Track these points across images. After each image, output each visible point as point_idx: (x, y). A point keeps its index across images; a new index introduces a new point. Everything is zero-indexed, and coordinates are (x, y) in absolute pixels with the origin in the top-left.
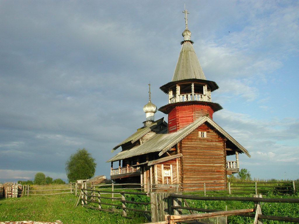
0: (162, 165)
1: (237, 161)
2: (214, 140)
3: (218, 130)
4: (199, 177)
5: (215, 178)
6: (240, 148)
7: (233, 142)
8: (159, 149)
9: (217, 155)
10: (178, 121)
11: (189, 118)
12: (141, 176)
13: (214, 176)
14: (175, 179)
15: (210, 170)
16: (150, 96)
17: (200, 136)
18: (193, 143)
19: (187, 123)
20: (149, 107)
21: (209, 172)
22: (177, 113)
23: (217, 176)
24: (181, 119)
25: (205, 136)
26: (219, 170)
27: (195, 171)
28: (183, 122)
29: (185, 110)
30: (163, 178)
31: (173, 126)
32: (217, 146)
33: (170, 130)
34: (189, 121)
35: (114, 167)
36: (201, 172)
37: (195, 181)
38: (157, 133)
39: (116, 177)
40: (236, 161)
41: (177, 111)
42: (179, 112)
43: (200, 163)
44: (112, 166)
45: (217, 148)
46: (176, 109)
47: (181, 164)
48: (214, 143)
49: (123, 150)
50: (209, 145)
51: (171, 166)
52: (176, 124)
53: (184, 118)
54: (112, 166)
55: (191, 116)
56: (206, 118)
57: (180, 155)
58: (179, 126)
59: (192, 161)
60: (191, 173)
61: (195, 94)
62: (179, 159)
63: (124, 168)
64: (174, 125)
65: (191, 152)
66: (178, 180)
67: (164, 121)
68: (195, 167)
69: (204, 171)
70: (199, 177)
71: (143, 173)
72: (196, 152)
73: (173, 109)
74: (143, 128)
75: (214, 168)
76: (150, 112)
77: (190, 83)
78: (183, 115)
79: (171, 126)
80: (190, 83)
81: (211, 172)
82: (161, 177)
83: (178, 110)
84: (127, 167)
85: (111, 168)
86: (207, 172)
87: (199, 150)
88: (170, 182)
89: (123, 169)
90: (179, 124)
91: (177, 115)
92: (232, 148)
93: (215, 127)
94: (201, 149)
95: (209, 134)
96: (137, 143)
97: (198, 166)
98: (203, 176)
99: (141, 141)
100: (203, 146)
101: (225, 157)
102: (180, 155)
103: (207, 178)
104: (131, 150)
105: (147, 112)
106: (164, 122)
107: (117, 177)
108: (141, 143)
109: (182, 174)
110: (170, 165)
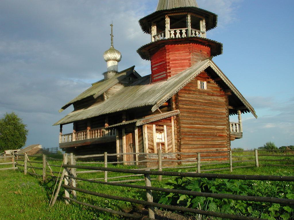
0: (154, 126)
1: (239, 122)
2: (215, 93)
3: (223, 79)
5: (218, 145)
6: (246, 106)
7: (239, 97)
8: (150, 101)
9: (219, 114)
10: (169, 66)
11: (185, 61)
12: (118, 142)
13: (216, 142)
14: (170, 147)
15: (212, 134)
16: (112, 40)
17: (199, 87)
18: (191, 96)
19: (182, 68)
20: (112, 54)
23: (219, 143)
24: (174, 62)
25: (205, 88)
26: (222, 134)
27: (194, 135)
29: (179, 51)
30: (155, 145)
31: (161, 72)
32: (218, 102)
34: (185, 66)
35: (64, 132)
36: (202, 137)
37: (194, 148)
38: (126, 85)
40: (239, 123)
42: (170, 53)
43: (200, 124)
44: (61, 130)
45: (218, 104)
46: (166, 48)
47: (177, 125)
48: (216, 98)
50: (209, 100)
51: (165, 126)
52: (166, 70)
53: (177, 62)
54: (61, 130)
55: (187, 59)
56: (209, 61)
58: (170, 72)
59: (191, 121)
60: (190, 138)
62: (175, 118)
63: (82, 133)
64: (164, 71)
66: (174, 147)
67: (135, 71)
68: (194, 129)
69: (204, 135)
70: (198, 143)
71: (121, 138)
72: (196, 109)
73: (161, 49)
74: (102, 81)
75: (216, 132)
76: (114, 60)
77: (184, 14)
78: (176, 57)
80: (184, 14)
81: (213, 137)
82: (152, 144)
83: (169, 49)
84: (88, 131)
85: (60, 133)
86: (208, 137)
87: (198, 106)
89: (80, 134)
90: (170, 69)
92: (237, 105)
93: (219, 75)
94: (201, 105)
95: (210, 85)
96: (101, 98)
97: (198, 128)
98: (204, 143)
100: (203, 101)
101: (228, 117)
102: (177, 112)
103: (208, 144)
105: (109, 60)
106: (134, 71)
108: (106, 99)
110: (163, 126)
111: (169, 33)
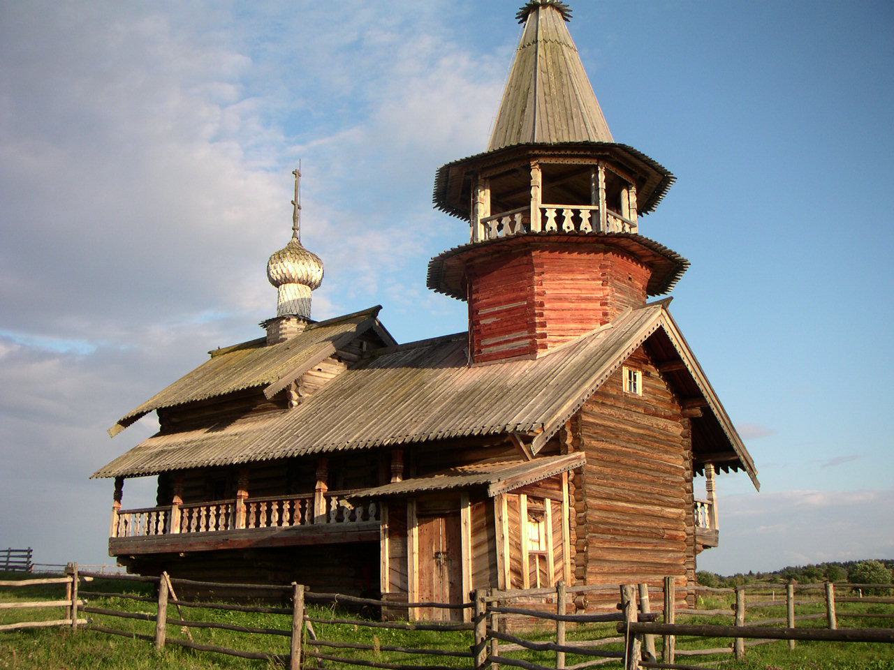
0: (524, 497)
1: (711, 500)
2: (661, 407)
3: (690, 368)
4: (624, 557)
5: (665, 564)
6: (738, 452)
7: (722, 423)
8: (518, 419)
9: (670, 473)
10: (541, 315)
11: (591, 305)
12: (385, 545)
13: (664, 555)
14: (559, 565)
15: (654, 531)
16: (295, 219)
17: (626, 387)
18: (607, 411)
19: (580, 326)
20: (301, 262)
21: (651, 540)
22: (536, 278)
23: (669, 559)
24: (557, 305)
25: (639, 391)
26: (674, 533)
27: (616, 532)
28: (562, 320)
29: (572, 272)
30: (526, 559)
31: (509, 332)
32: (667, 435)
33: (485, 351)
34: (589, 320)
35: (126, 504)
36: (631, 539)
37: (614, 574)
38: (352, 365)
39: (159, 545)
40: (710, 502)
41: (537, 270)
42: (545, 276)
43: (628, 501)
44: (118, 496)
45: (667, 443)
46: (535, 261)
47: (577, 501)
48: (662, 423)
49: (164, 431)
50: (648, 428)
51: (548, 501)
52: (532, 326)
53: (567, 305)
54: (118, 496)
55: (597, 299)
56: (659, 313)
57: (577, 458)
58: (544, 336)
59: (607, 490)
60: (605, 541)
61: (610, 211)
62: (571, 477)
63: (213, 509)
64: (522, 329)
65: (604, 451)
66: (568, 568)
67: (380, 323)
68: (614, 515)
69: (636, 534)
70: (624, 557)
71: (399, 533)
72: (619, 453)
73: (514, 262)
74: (261, 343)
75: (663, 525)
76: (301, 282)
77: (588, 162)
78: (563, 291)
79: (492, 335)
80: (588, 162)
81: (655, 541)
82: (518, 555)
83: (541, 265)
84: (241, 505)
85: (116, 504)
86: (645, 540)
87: (624, 444)
88: (544, 576)
89: (204, 513)
90: (543, 325)
91: (536, 289)
92: (714, 446)
93: (682, 355)
94: (629, 441)
95: (650, 382)
96: (282, 401)
97: (623, 512)
98: (635, 557)
99: (293, 392)
100: (635, 430)
101: (689, 481)
102: (579, 458)
103: (644, 563)
104: (232, 430)
105: (287, 280)
106: (377, 324)
107: (144, 545)
108: (295, 403)
109: (581, 547)
110: (542, 500)
111: (542, 215)
